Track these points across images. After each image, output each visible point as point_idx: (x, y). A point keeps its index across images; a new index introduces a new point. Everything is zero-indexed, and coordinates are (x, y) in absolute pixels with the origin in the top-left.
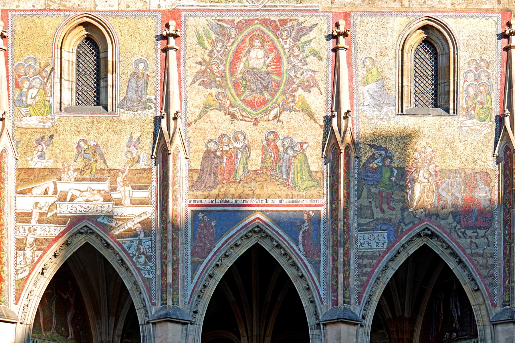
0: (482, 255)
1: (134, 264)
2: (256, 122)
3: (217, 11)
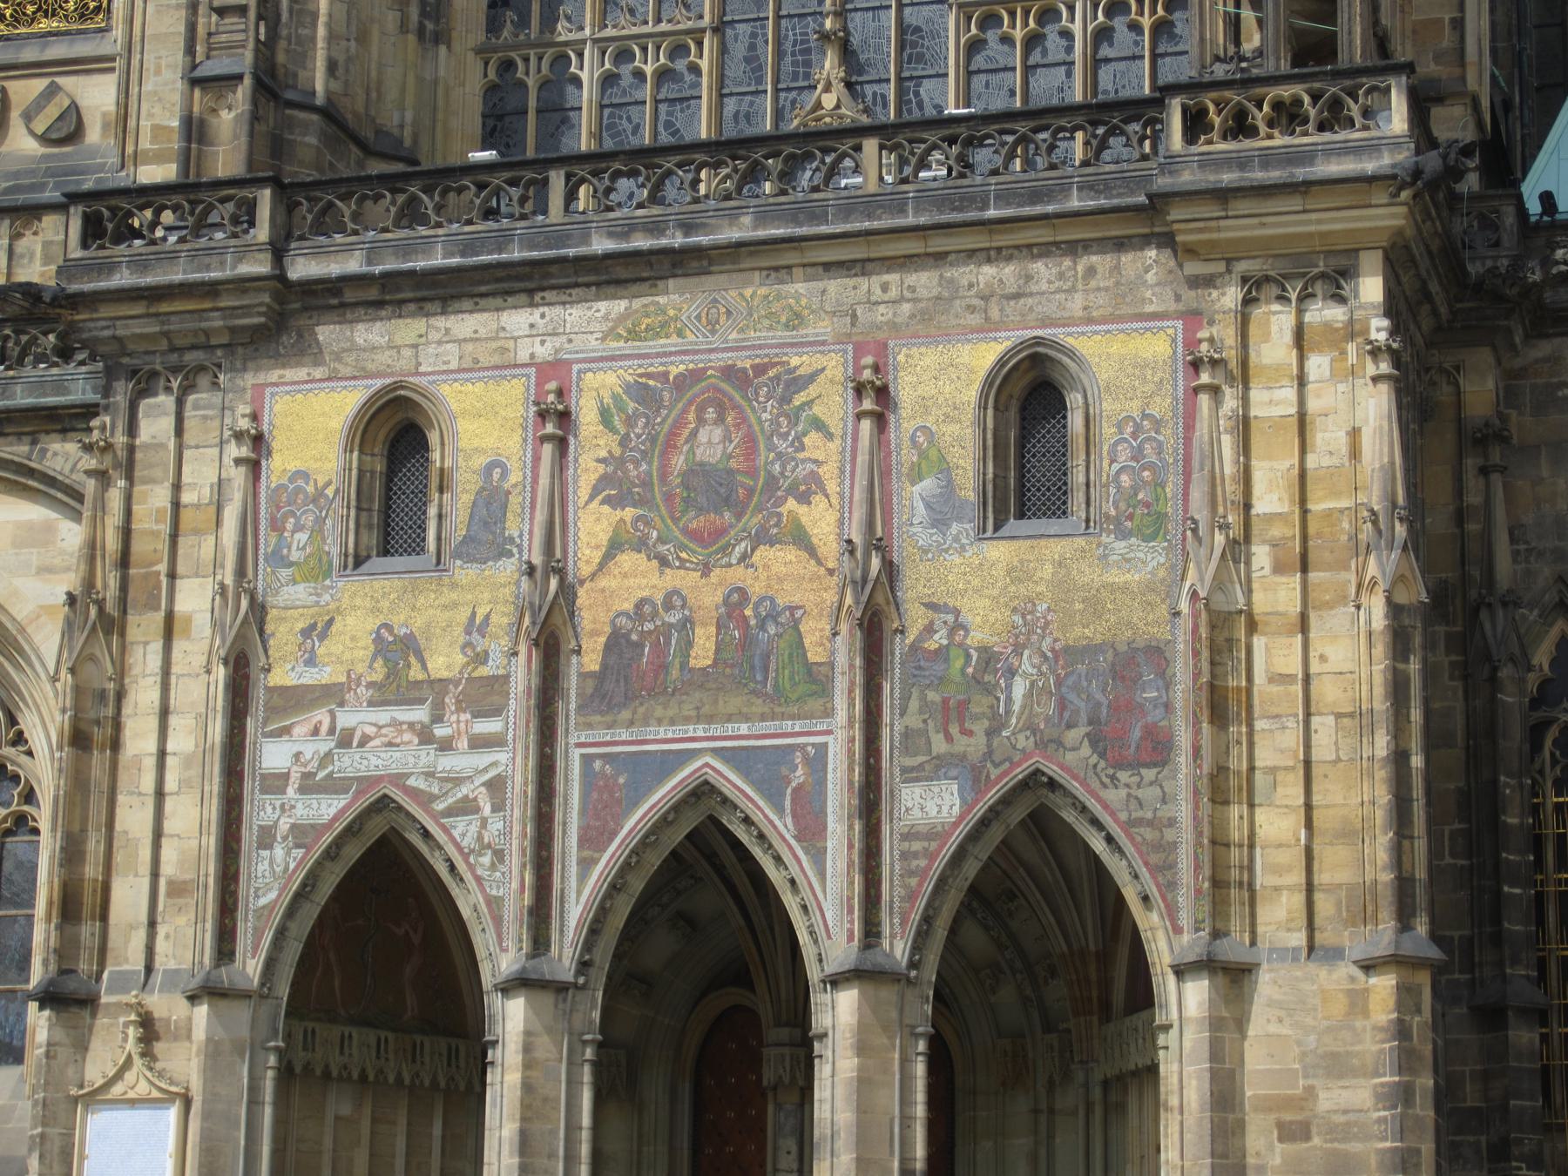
0: (1150, 823)
1: (472, 868)
2: (706, 570)
3: (639, 356)
